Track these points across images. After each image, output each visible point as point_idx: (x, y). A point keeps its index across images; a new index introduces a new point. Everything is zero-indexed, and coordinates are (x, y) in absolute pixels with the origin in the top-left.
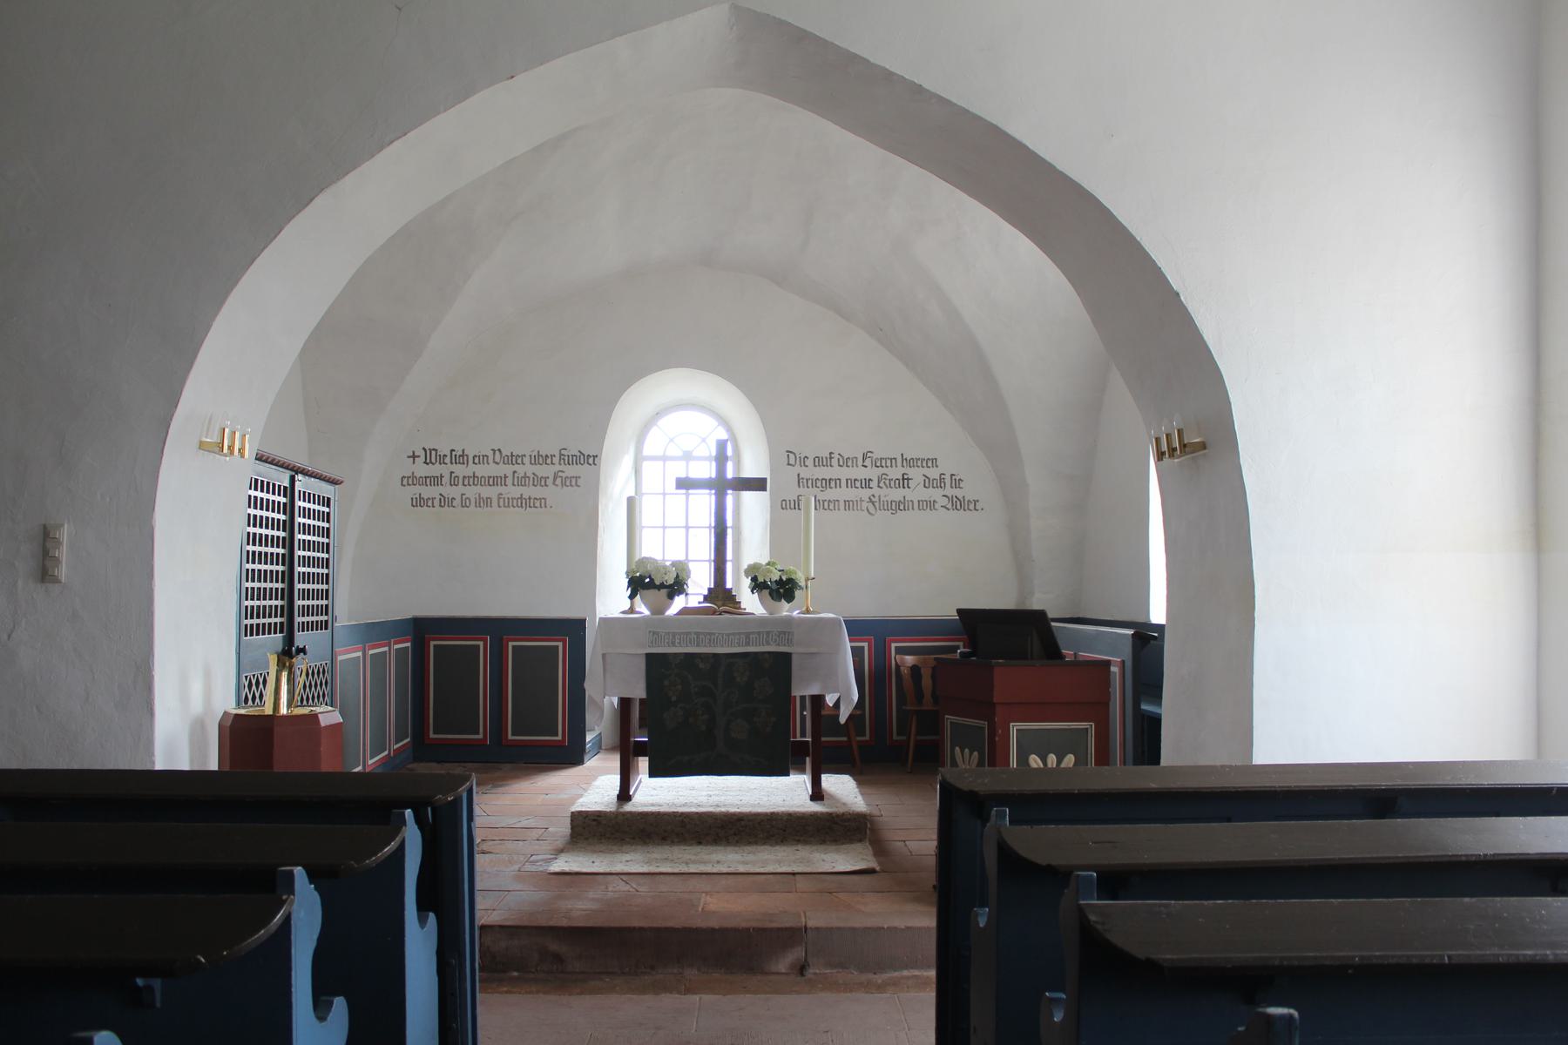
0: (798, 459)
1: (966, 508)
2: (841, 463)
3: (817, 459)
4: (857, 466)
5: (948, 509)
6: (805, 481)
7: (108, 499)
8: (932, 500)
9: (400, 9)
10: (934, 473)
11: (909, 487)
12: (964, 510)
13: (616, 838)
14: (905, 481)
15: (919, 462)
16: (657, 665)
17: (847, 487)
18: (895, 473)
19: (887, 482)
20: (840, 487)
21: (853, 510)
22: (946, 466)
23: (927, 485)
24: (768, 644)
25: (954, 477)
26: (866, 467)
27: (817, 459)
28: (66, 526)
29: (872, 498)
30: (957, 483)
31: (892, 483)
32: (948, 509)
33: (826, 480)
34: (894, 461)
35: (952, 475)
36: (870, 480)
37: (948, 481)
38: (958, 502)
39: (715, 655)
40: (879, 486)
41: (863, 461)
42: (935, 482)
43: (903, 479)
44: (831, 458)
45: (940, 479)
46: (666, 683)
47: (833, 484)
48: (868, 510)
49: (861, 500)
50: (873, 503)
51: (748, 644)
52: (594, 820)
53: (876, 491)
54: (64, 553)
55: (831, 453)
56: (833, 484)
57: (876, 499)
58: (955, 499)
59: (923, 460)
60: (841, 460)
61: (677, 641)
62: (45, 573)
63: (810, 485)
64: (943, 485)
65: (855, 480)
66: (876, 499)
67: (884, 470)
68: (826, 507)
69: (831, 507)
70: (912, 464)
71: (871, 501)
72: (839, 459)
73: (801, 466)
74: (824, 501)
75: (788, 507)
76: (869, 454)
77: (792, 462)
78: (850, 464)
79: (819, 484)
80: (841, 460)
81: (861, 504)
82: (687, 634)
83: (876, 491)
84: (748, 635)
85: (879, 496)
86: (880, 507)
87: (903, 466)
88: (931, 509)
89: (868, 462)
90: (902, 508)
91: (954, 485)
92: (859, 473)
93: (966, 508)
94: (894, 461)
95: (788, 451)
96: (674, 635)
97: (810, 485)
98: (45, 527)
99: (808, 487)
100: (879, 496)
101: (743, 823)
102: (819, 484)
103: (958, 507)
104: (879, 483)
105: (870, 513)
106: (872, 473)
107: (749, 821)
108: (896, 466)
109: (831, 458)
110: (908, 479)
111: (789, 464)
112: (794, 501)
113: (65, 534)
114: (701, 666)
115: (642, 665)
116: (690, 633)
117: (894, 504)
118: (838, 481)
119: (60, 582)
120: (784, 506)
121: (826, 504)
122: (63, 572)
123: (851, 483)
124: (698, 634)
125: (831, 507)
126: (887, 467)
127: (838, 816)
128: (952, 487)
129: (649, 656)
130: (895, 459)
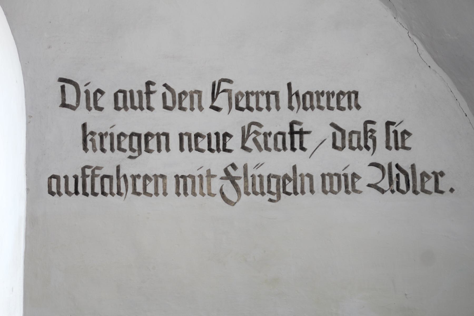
0: (83, 96)
1: (419, 189)
2: (169, 103)
3: (121, 96)
4: (201, 108)
5: (383, 191)
6: (97, 138)
8: (349, 172)
11: (303, 149)
12: (415, 192)
17: (182, 149)
19: (261, 139)
20: (168, 149)
21: (194, 194)
23: (339, 144)
25: (392, 128)
26: (217, 109)
27: (121, 96)
29: (230, 169)
31: (271, 141)
32: (383, 191)
33: (139, 136)
34: (272, 97)
35: (389, 124)
36: (226, 135)
38: (402, 177)
40: (244, 148)
41: (214, 99)
42: (355, 137)
43: (292, 133)
44: (149, 93)
45: (366, 132)
47: (153, 144)
48: (222, 194)
49: (210, 176)
50: (233, 180)
55: (149, 84)
56: (153, 144)
57: (239, 173)
58: (395, 171)
59: (330, 95)
60: (169, 95)
63: (107, 145)
64: (370, 143)
65: (198, 135)
66: (239, 173)
67: (255, 116)
70: (308, 105)
72: (164, 95)
73: (89, 109)
74: (134, 178)
75: (63, 190)
76: (224, 86)
77: (71, 99)
78: (186, 103)
79: (125, 144)
80: (169, 95)
81: (209, 184)
85: (245, 167)
86: (246, 187)
87: (291, 108)
88: (347, 192)
89: (222, 100)
90: (289, 188)
91: (392, 144)
93: (419, 189)
94: (272, 97)
95: (61, 80)
97: (107, 145)
99: (103, 150)
100: (245, 167)
102: (125, 144)
103: (403, 186)
104: (244, 140)
108: (278, 108)
110: (301, 133)
111: (64, 105)
112: (76, 178)
117: (274, 181)
118: (163, 138)
120: (54, 189)
121: (139, 183)
125: (151, 188)
126: (259, 109)
128: (388, 147)
130: (276, 94)
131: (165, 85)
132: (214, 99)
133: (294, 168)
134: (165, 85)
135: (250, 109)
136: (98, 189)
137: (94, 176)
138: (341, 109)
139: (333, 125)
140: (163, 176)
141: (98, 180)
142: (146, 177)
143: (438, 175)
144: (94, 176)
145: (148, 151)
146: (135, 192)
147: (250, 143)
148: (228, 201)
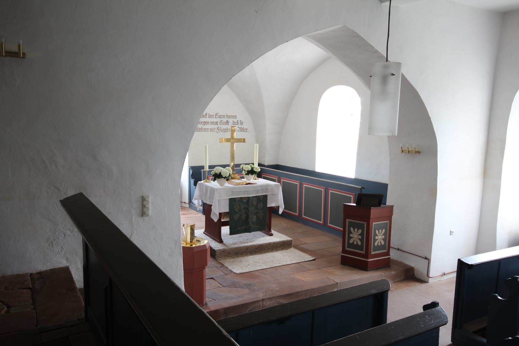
4: (214, 118)
7: (164, 185)
9: (257, 12)
10: (235, 120)
13: (229, 256)
14: (227, 122)
15: (232, 117)
16: (232, 201)
18: (225, 120)
19: (222, 123)
22: (239, 118)
24: (263, 193)
26: (216, 118)
28: (150, 197)
30: (242, 123)
31: (224, 123)
32: (239, 131)
35: (241, 121)
37: (239, 123)
39: (248, 197)
40: (220, 124)
41: (216, 116)
43: (227, 122)
44: (206, 115)
46: (235, 207)
48: (217, 132)
49: (215, 129)
50: (218, 129)
51: (257, 193)
52: (223, 252)
53: (219, 126)
54: (150, 206)
58: (241, 128)
59: (232, 116)
61: (239, 194)
62: (143, 214)
65: (213, 122)
68: (205, 131)
69: (206, 131)
71: (218, 129)
74: (204, 129)
76: (217, 114)
78: (212, 117)
82: (242, 191)
83: (219, 126)
84: (257, 191)
85: (220, 127)
89: (217, 116)
90: (226, 131)
92: (214, 120)
96: (238, 192)
98: (142, 196)
101: (262, 247)
103: (242, 131)
105: (218, 133)
106: (218, 120)
107: (264, 246)
108: (225, 118)
109: (206, 115)
110: (228, 122)
113: (150, 199)
114: (244, 201)
115: (228, 202)
116: (242, 191)
119: (149, 216)
122: (150, 212)
123: (212, 123)
124: (244, 191)
125: (206, 131)
126: (222, 118)
127: (285, 241)
129: (230, 200)
131: (209, 114)
132: (216, 116)
133: (227, 128)
134: (209, 114)
135: (221, 118)
136: (199, 131)
137: (198, 129)
138: (234, 118)
139: (233, 121)
140: (208, 129)
141: (199, 129)
142: (206, 129)
143: (247, 129)
144: (198, 129)
145: (206, 125)
146: (204, 131)
147: (221, 124)
148: (218, 133)
